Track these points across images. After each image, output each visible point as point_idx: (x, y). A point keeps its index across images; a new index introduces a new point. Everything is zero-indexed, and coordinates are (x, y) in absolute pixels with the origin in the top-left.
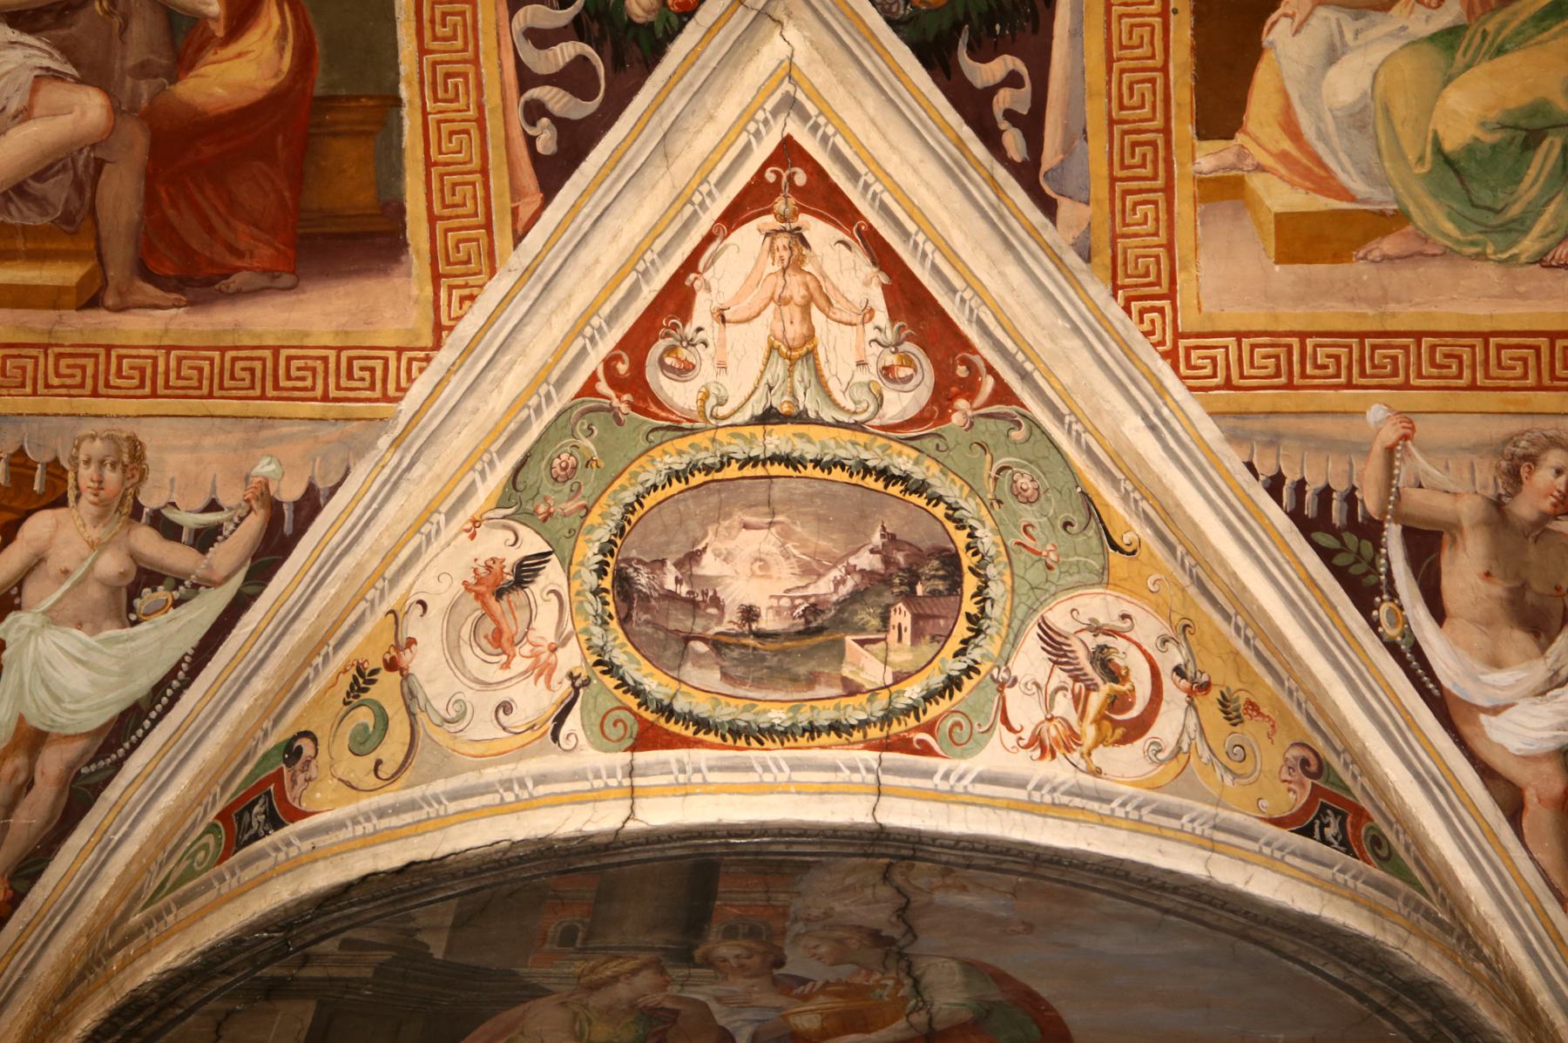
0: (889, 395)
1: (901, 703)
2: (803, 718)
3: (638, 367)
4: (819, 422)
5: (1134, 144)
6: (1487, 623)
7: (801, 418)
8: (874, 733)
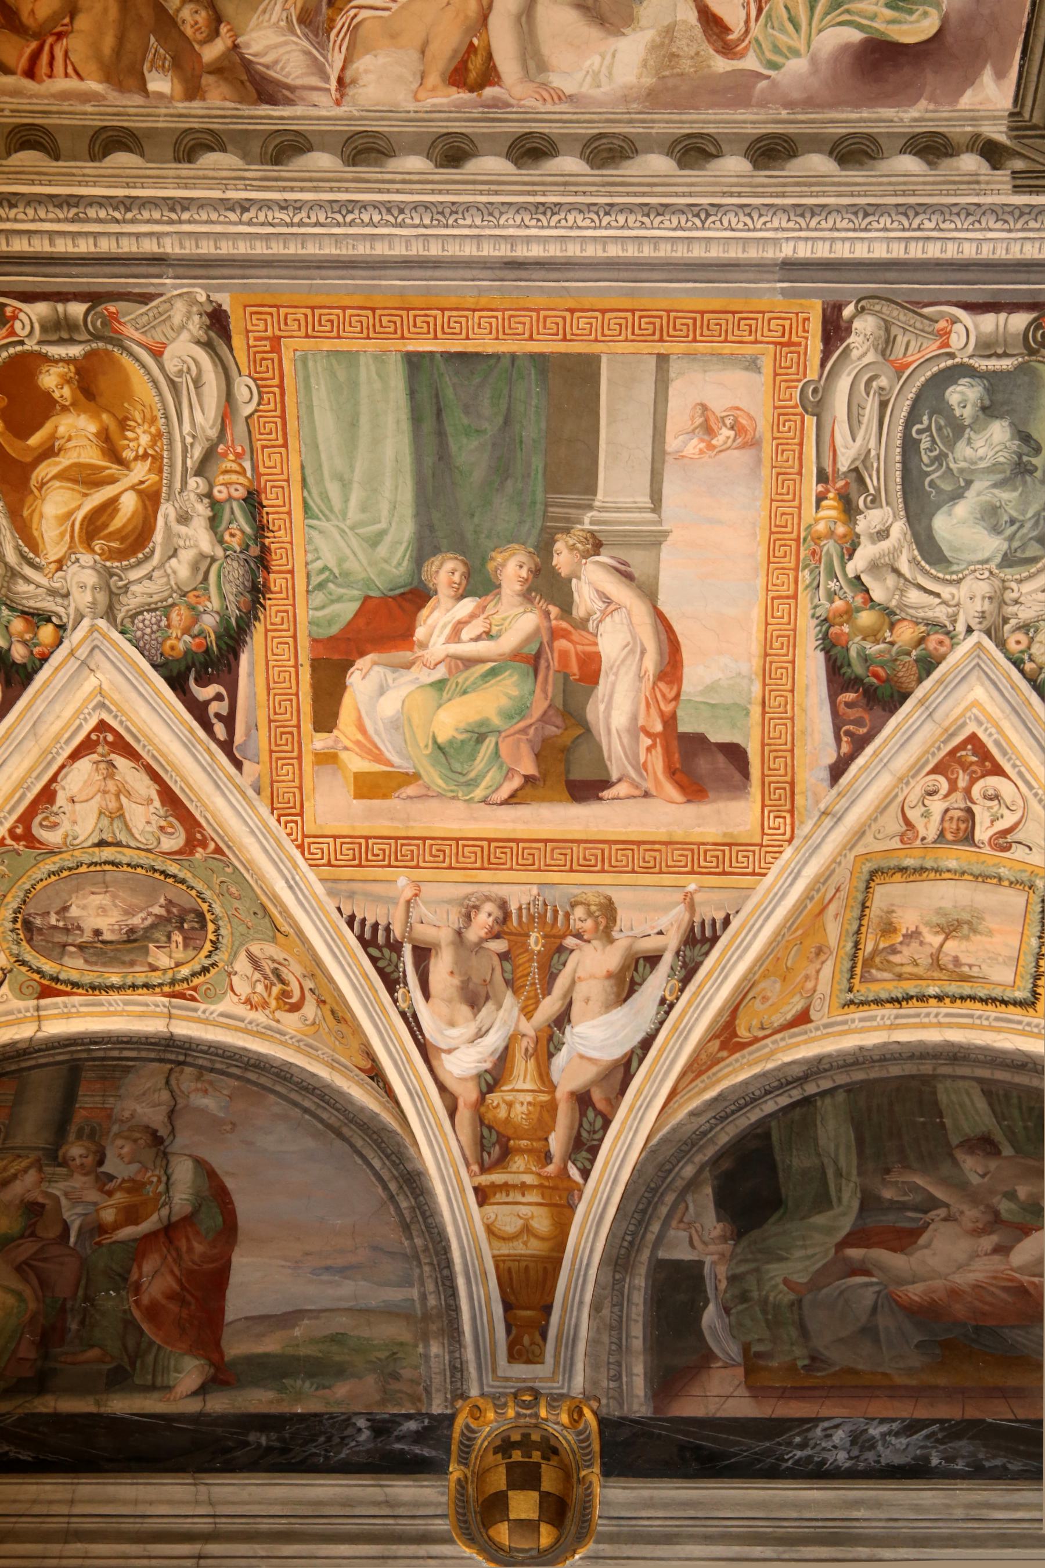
0: (163, 839)
1: (179, 976)
2: (129, 980)
3: (28, 829)
4: (128, 847)
5: (282, 733)
6: (450, 1001)
7: (119, 844)
8: (166, 989)
